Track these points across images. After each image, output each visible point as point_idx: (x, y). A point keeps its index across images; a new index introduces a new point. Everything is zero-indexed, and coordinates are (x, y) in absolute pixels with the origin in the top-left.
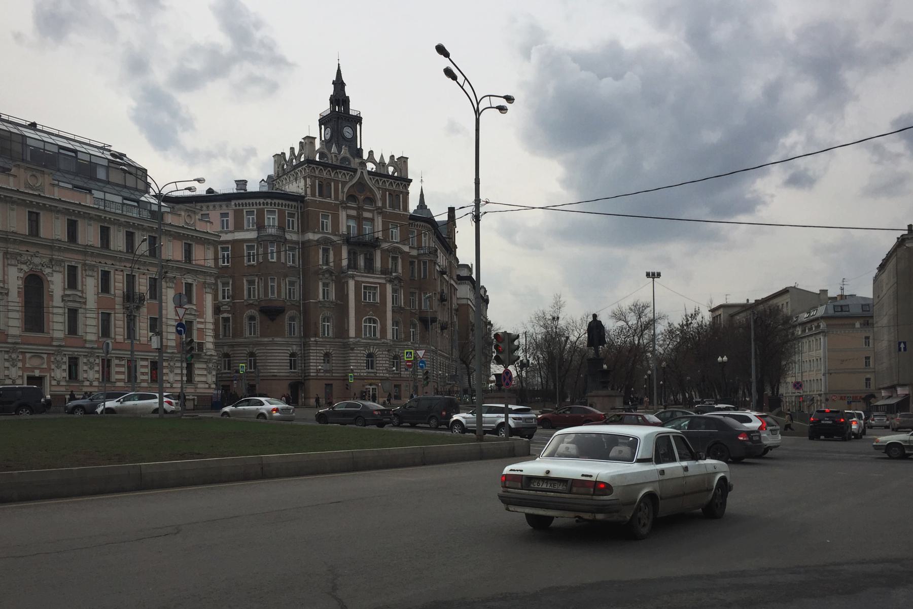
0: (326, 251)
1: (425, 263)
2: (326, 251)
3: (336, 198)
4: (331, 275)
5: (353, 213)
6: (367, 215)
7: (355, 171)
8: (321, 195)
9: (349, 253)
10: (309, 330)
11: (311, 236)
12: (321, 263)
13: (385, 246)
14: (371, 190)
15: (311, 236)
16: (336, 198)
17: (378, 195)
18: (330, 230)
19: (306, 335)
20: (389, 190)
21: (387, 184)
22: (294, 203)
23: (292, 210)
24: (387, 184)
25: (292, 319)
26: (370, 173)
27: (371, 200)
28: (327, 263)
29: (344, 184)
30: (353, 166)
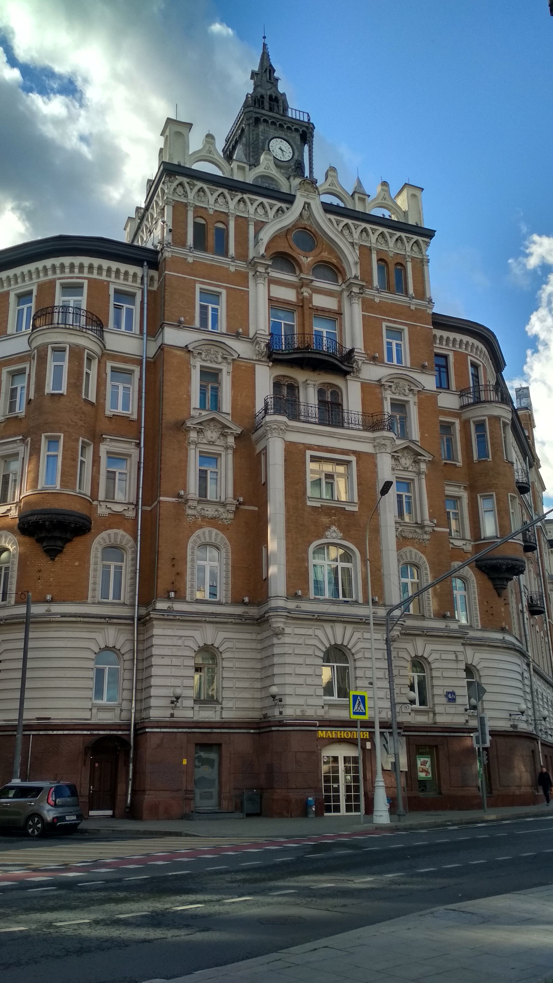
0: (210, 376)
1: (480, 426)
2: (210, 376)
3: (242, 255)
4: (224, 435)
5: (290, 295)
6: (319, 301)
7: (289, 199)
8: (200, 243)
9: (277, 385)
10: (155, 581)
11: (173, 336)
12: (195, 401)
13: (372, 373)
14: (333, 247)
15: (173, 336)
16: (242, 255)
17: (351, 256)
18: (223, 326)
19: (147, 593)
20: (379, 251)
21: (373, 238)
22: (132, 269)
23: (128, 286)
24: (373, 238)
25: (113, 550)
26: (328, 208)
27: (332, 269)
28: (216, 405)
29: (260, 226)
30: (285, 189)
